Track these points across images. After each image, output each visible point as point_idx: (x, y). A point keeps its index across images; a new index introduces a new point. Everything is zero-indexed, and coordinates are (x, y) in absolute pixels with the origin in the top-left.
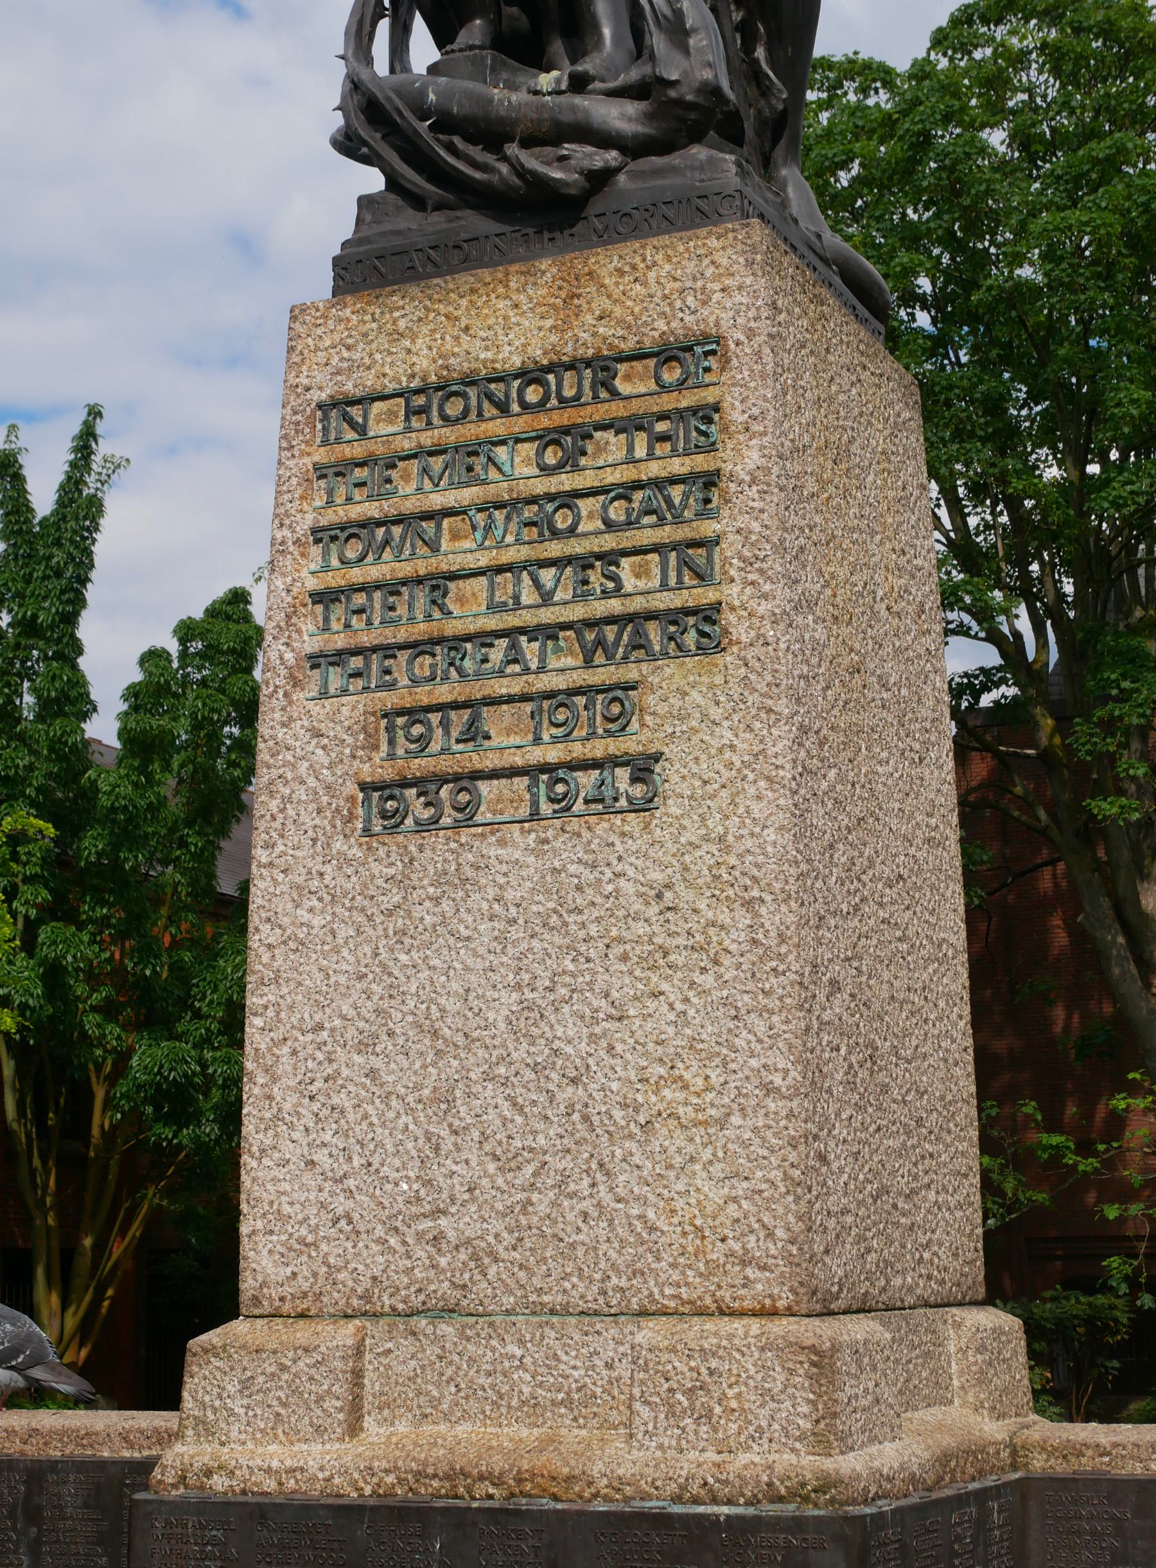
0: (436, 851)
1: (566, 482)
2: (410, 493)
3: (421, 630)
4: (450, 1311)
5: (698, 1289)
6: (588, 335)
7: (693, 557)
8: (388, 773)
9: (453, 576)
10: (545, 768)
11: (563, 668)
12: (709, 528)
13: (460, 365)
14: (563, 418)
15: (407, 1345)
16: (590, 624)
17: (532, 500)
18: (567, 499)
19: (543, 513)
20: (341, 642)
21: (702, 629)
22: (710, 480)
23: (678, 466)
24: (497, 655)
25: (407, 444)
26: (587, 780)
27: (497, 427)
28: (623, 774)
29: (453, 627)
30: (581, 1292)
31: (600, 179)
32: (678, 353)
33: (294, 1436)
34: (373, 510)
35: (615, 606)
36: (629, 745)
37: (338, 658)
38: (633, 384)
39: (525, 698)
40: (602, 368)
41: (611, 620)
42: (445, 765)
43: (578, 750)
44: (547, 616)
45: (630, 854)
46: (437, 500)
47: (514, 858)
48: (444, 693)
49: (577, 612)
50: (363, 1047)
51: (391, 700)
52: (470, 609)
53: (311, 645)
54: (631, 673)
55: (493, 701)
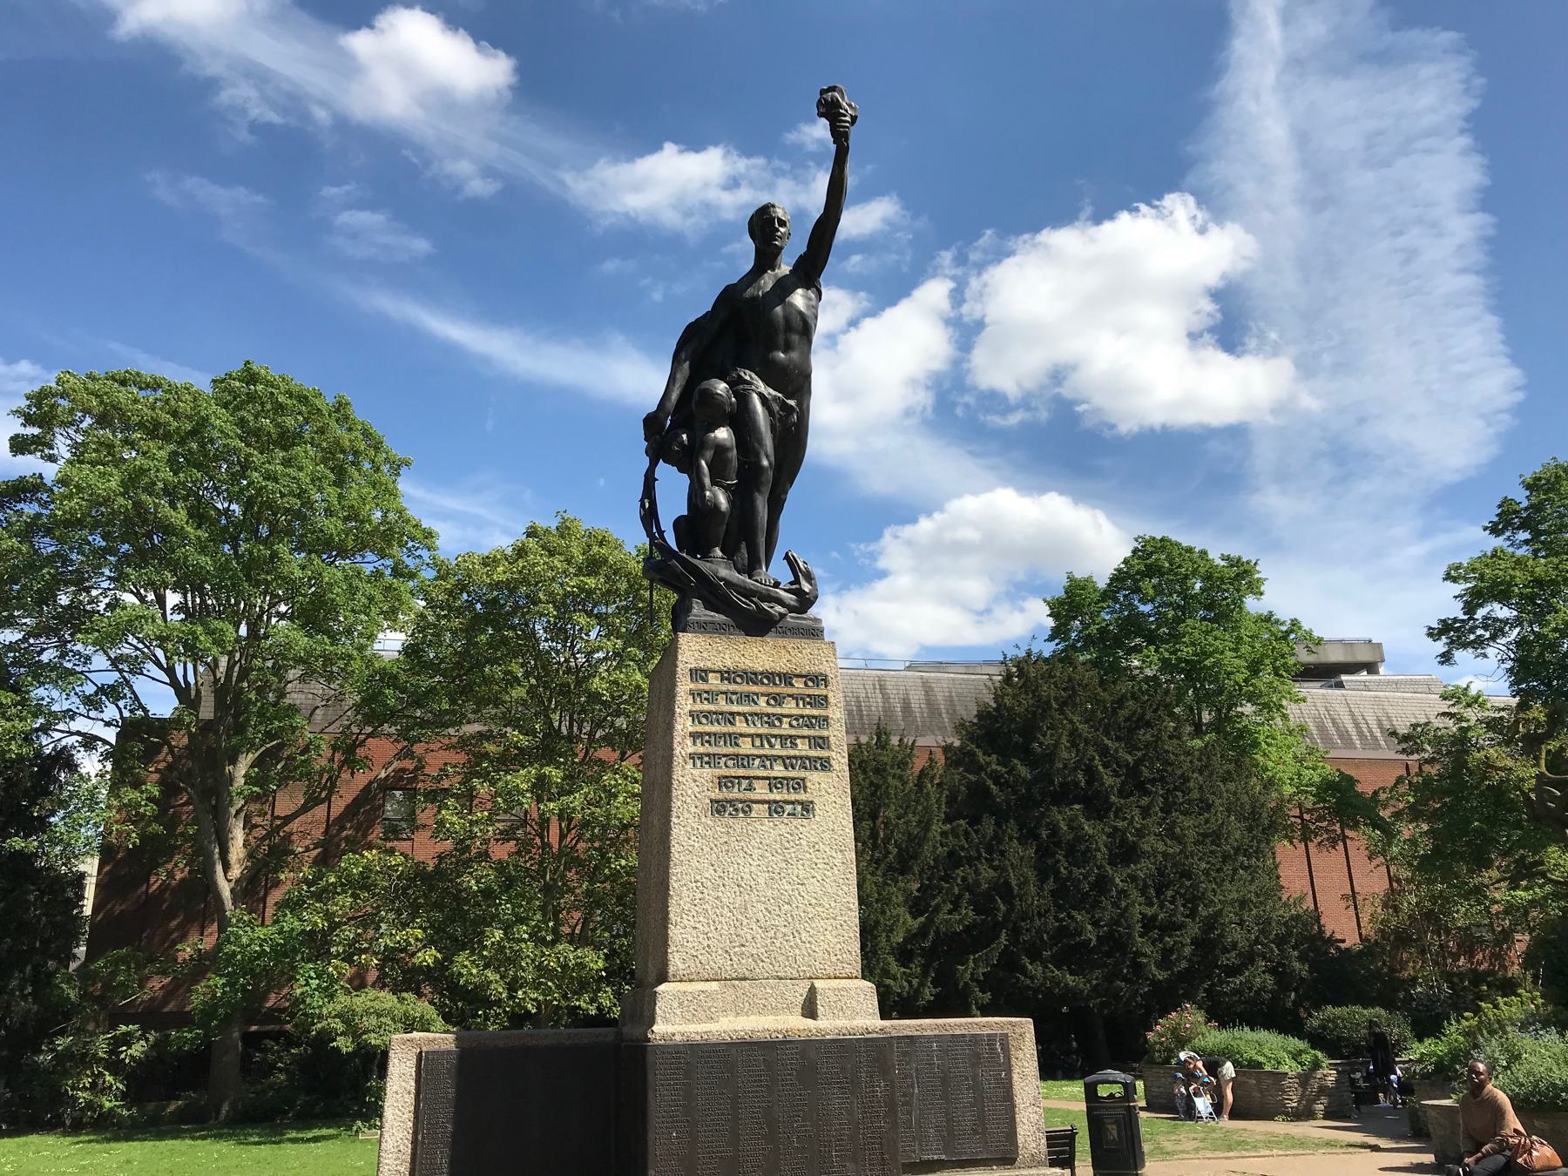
0: (739, 824)
1: (778, 710)
2: (722, 705)
3: (730, 750)
4: (745, 979)
5: (830, 971)
6: (781, 665)
7: (822, 742)
8: (721, 797)
9: (742, 735)
10: (776, 802)
11: (779, 770)
12: (825, 733)
13: (742, 666)
14: (777, 690)
15: (731, 991)
16: (789, 758)
17: (768, 715)
18: (780, 717)
19: (771, 719)
20: (701, 750)
21: (825, 765)
22: (826, 719)
23: (815, 712)
24: (757, 761)
25: (724, 688)
26: (789, 808)
27: (755, 689)
28: (799, 808)
29: (741, 751)
30: (790, 972)
31: (782, 616)
32: (817, 679)
33: (700, 1021)
34: (712, 708)
35: (797, 753)
36: (802, 797)
37: (701, 756)
38: (799, 684)
39: (767, 778)
40: (787, 678)
41: (795, 757)
42: (741, 796)
43: (786, 797)
44: (774, 752)
45: (807, 829)
46: (735, 708)
47: (765, 830)
48: (741, 772)
49: (784, 753)
50: (716, 889)
51: (718, 772)
52: (746, 747)
53: (691, 750)
54: (802, 774)
55: (758, 778)
